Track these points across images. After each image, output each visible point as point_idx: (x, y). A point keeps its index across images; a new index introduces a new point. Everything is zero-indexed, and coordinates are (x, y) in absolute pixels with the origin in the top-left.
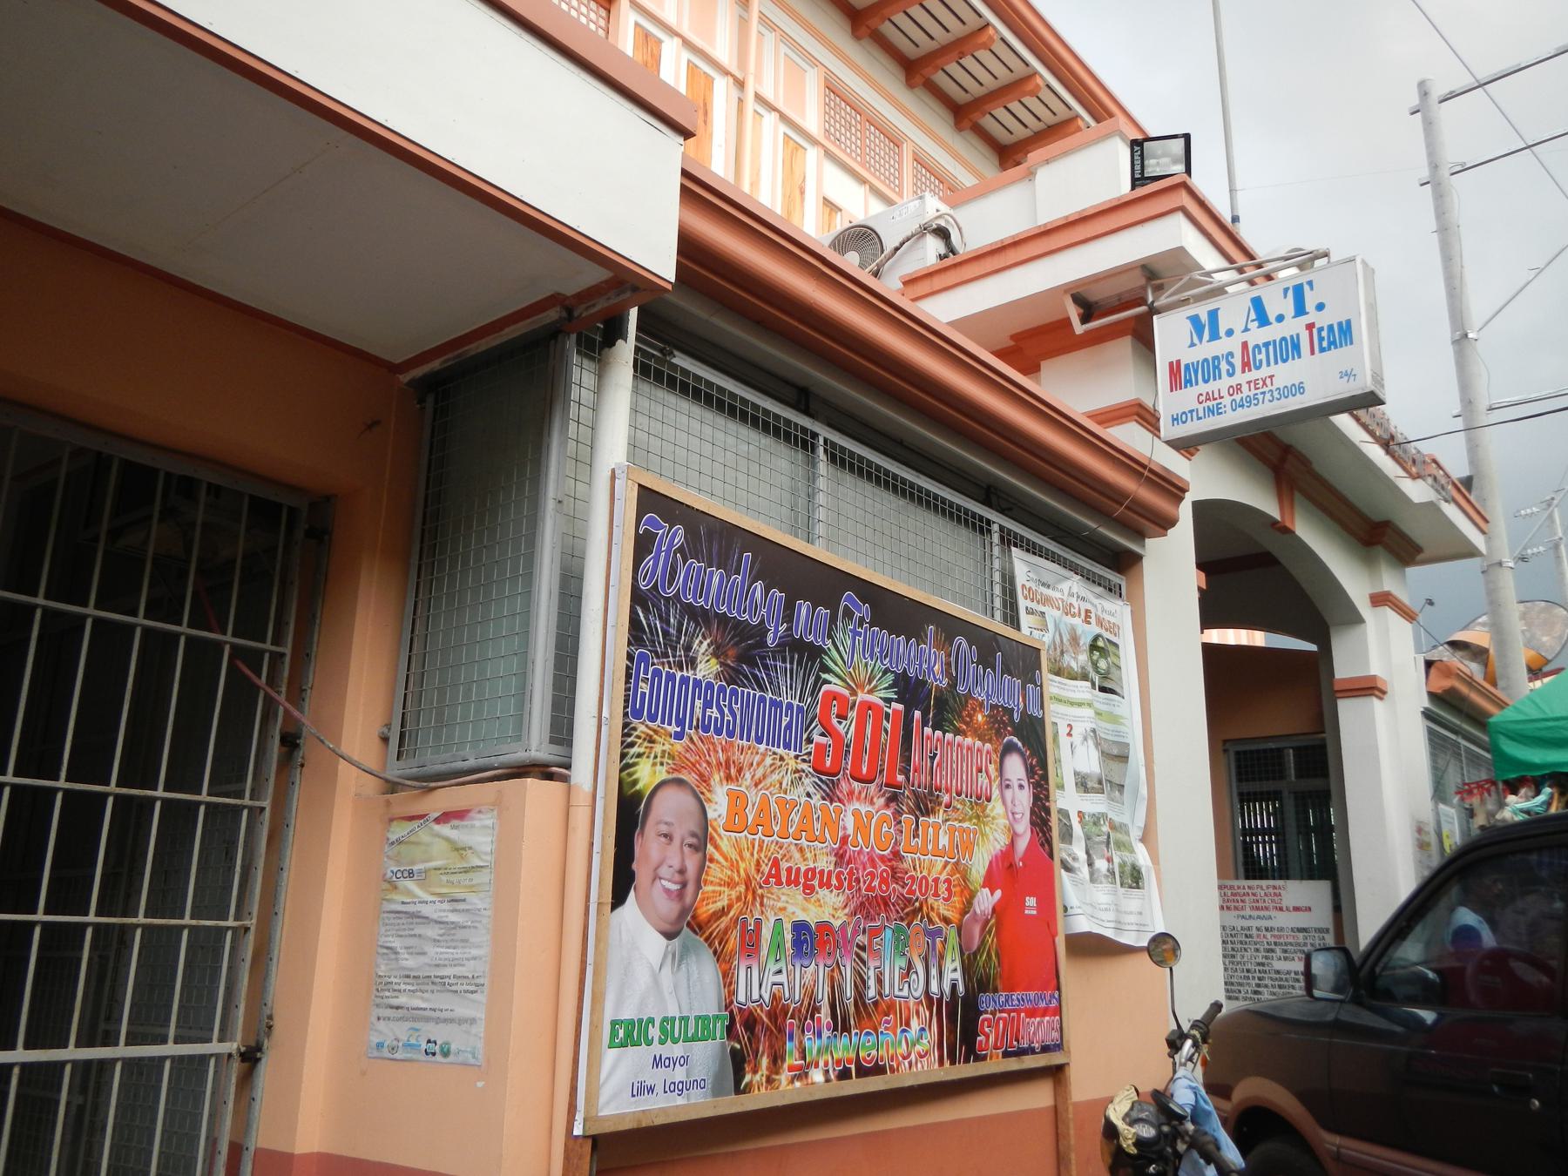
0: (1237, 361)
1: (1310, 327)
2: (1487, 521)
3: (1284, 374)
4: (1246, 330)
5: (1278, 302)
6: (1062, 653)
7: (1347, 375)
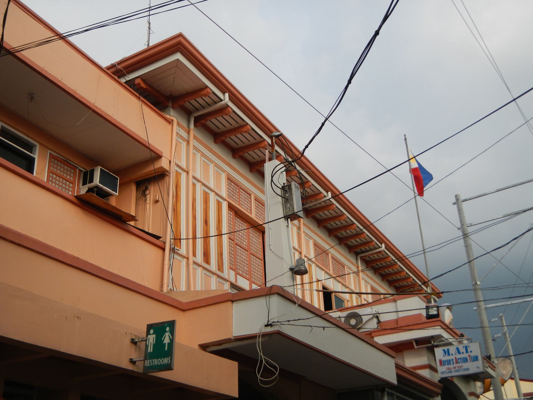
0: (454, 361)
1: (469, 356)
3: (465, 365)
5: (462, 350)
7: (478, 367)
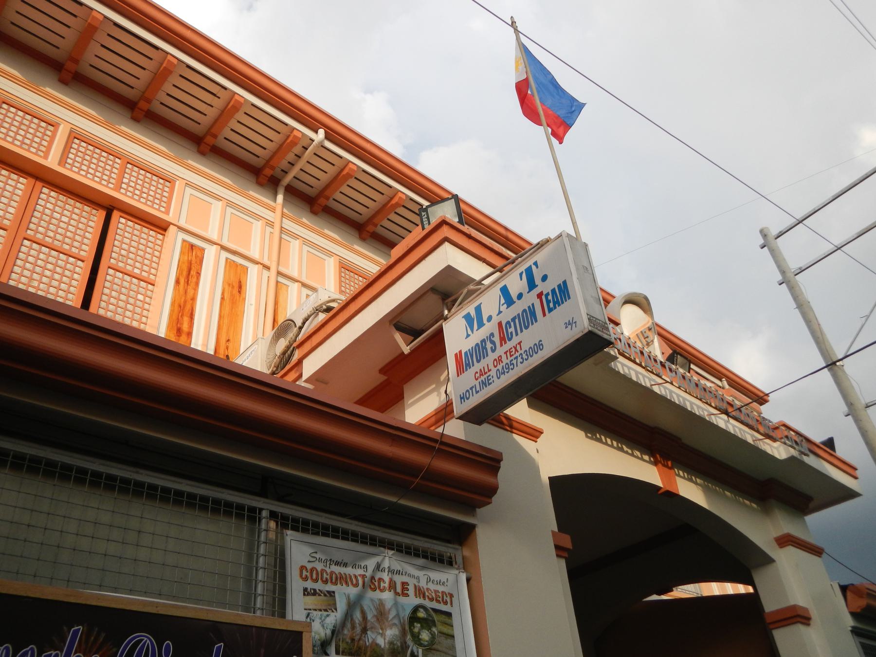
0: (497, 339)
1: (540, 296)
2: (855, 469)
3: (527, 338)
4: (500, 312)
6: (364, 630)
7: (570, 324)
